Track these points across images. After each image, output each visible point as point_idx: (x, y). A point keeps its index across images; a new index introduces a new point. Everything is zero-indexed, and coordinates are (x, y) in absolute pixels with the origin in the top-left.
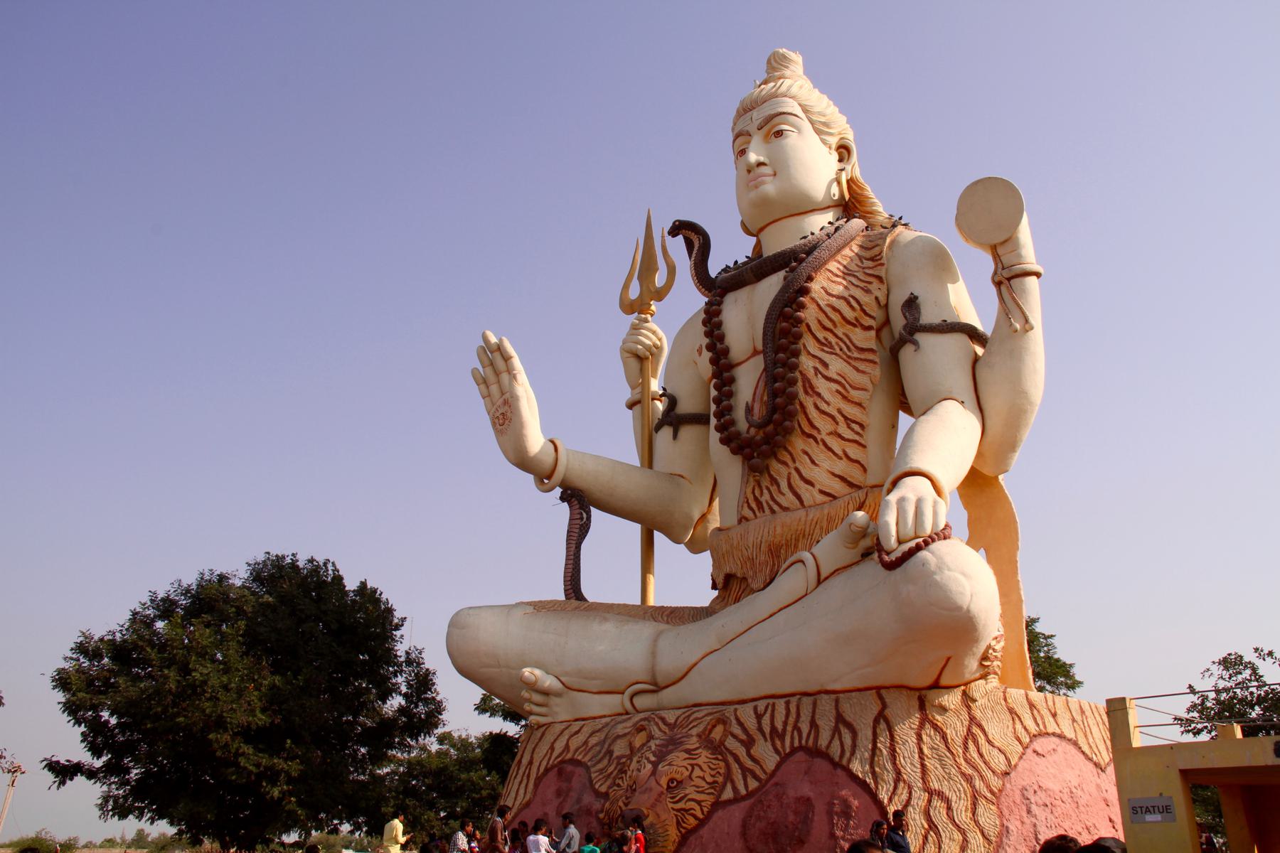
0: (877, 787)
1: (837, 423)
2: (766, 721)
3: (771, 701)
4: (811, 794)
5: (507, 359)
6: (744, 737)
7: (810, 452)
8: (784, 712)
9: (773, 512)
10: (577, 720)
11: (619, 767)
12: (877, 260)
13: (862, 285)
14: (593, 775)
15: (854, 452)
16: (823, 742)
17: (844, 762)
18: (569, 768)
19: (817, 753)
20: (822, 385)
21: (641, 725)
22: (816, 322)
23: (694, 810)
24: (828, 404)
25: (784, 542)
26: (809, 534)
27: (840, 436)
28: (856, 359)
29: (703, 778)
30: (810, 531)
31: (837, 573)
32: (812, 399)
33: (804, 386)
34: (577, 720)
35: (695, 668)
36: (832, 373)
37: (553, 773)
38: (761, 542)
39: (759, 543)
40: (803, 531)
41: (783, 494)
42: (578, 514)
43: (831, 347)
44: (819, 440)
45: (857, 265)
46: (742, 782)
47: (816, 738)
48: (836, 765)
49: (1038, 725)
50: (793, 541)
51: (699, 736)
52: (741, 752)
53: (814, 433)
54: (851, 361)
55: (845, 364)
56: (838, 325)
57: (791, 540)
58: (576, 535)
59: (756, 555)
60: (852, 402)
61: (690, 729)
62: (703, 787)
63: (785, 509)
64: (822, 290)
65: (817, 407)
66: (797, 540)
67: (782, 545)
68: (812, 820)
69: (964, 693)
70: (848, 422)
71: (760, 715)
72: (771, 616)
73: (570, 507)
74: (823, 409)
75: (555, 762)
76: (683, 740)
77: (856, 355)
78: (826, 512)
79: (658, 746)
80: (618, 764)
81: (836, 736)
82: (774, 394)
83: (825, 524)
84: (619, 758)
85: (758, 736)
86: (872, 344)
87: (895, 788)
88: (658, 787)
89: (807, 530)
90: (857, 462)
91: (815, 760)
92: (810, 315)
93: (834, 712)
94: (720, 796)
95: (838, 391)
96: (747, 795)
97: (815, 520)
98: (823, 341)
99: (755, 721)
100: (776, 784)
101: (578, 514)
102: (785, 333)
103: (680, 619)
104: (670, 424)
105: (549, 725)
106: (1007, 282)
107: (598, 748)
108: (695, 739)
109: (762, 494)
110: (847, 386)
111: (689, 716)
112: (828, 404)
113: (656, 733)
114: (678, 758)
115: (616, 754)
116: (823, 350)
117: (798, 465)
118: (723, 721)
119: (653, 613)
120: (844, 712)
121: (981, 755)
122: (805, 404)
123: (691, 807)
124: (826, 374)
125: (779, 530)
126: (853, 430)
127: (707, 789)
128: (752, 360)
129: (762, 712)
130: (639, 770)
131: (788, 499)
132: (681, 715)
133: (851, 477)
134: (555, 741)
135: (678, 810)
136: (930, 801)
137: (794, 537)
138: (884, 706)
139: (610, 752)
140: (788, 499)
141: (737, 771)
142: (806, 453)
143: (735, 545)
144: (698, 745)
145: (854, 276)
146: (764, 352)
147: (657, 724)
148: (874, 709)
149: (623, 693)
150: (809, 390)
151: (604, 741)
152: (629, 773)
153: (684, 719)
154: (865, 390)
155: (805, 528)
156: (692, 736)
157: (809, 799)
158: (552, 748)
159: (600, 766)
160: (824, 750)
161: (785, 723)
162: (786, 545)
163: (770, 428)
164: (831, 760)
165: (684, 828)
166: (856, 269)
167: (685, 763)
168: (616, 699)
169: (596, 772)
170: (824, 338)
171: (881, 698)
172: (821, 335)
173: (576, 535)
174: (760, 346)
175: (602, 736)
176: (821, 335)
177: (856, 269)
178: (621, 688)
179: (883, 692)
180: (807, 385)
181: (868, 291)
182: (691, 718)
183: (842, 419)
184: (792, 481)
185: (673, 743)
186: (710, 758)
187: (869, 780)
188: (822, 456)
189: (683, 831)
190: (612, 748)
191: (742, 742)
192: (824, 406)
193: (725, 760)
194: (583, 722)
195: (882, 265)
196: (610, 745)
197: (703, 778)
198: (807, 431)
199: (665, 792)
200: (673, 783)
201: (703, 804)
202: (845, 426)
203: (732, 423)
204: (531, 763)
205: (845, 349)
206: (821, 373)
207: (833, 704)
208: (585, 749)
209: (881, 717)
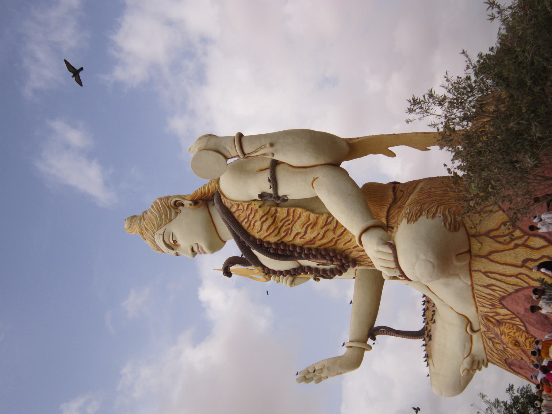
0: (521, 286)
1: (328, 230)
2: (487, 306)
6: (494, 314)
7: (345, 242)
13: (253, 213)
16: (498, 296)
19: (503, 298)
20: (310, 236)
22: (276, 237)
24: (319, 234)
28: (293, 217)
32: (317, 241)
33: (311, 244)
37: (512, 367)
43: (288, 229)
44: (338, 238)
45: (242, 212)
51: (494, 326)
53: (335, 240)
54: (295, 220)
55: (297, 223)
56: (276, 226)
64: (259, 234)
65: (321, 239)
69: (474, 236)
70: (327, 223)
72: (433, 293)
73: (378, 334)
74: (321, 237)
77: (291, 217)
86: (285, 210)
92: (273, 239)
93: (482, 287)
95: (312, 228)
98: (285, 233)
106: (246, 156)
108: (495, 328)
110: (308, 223)
112: (319, 234)
113: (492, 336)
115: (502, 349)
124: (303, 234)
136: (527, 267)
142: (345, 244)
145: (249, 215)
148: (481, 275)
149: (471, 336)
150: (312, 242)
154: (309, 216)
161: (487, 301)
169: (511, 357)
171: (476, 271)
180: (310, 243)
181: (257, 211)
182: (485, 325)
187: (517, 288)
188: (346, 237)
192: (320, 236)
193: (506, 323)
197: (515, 333)
198: (334, 244)
200: (517, 345)
205: (289, 222)
209: (485, 273)
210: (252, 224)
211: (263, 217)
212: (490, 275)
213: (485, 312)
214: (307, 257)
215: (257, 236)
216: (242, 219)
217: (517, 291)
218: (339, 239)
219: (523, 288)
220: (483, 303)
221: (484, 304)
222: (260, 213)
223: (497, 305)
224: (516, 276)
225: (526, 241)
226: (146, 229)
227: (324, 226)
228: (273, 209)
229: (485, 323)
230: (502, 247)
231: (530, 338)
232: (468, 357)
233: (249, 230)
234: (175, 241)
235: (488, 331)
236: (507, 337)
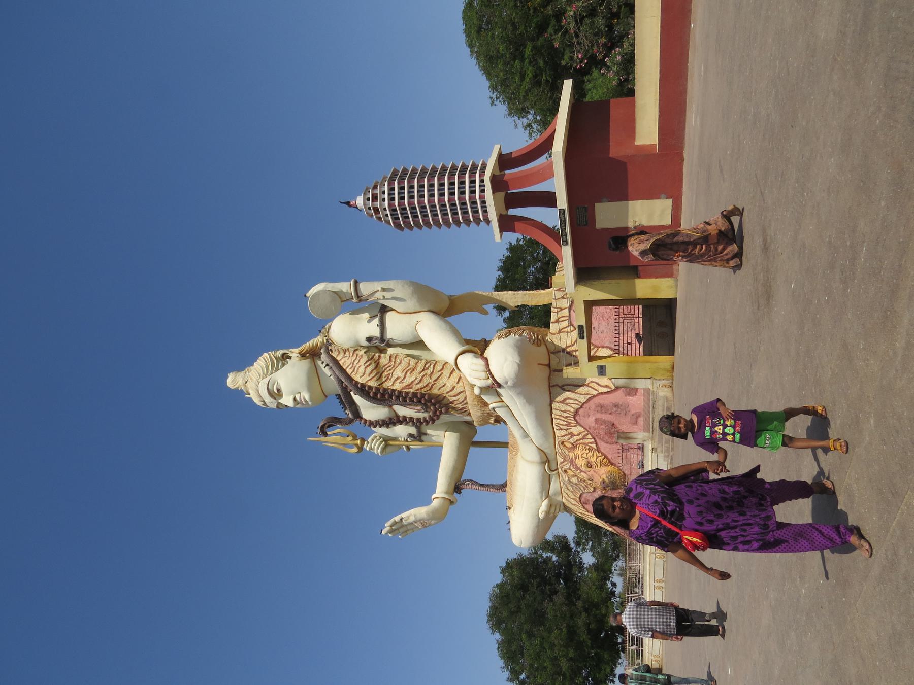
0: (591, 394)
1: (426, 374)
2: (563, 427)
4: (594, 418)
5: (395, 523)
6: (570, 436)
10: (562, 493)
15: (439, 367)
16: (572, 410)
18: (583, 500)
19: (576, 412)
20: (409, 380)
24: (416, 378)
29: (587, 454)
33: (409, 388)
36: (402, 376)
37: (586, 506)
43: (389, 374)
46: (589, 440)
47: (571, 412)
48: (582, 407)
51: (569, 452)
52: (576, 438)
53: (430, 385)
60: (416, 366)
65: (419, 383)
68: (605, 420)
69: (553, 353)
77: (393, 363)
80: (581, 481)
82: (411, 400)
85: (570, 431)
87: (592, 387)
92: (373, 384)
95: (411, 373)
96: (594, 439)
98: (386, 378)
102: (383, 395)
104: (420, 437)
108: (570, 454)
110: (408, 369)
112: (416, 378)
113: (567, 466)
115: (577, 482)
116: (391, 379)
117: (445, 392)
118: (563, 443)
122: (417, 388)
126: (428, 367)
135: (601, 465)
138: (557, 385)
139: (576, 484)
140: (462, 399)
142: (440, 389)
145: (354, 362)
147: (564, 465)
150: (410, 386)
157: (596, 419)
158: (575, 505)
159: (582, 488)
161: (564, 421)
164: (580, 408)
166: (350, 360)
167: (581, 460)
171: (554, 386)
172: (384, 379)
175: (569, 486)
176: (384, 379)
177: (349, 361)
179: (551, 385)
180: (407, 387)
181: (362, 356)
185: (572, 462)
187: (589, 396)
188: (441, 382)
189: (609, 464)
191: (571, 437)
192: (418, 381)
195: (348, 349)
197: (587, 454)
205: (390, 368)
212: (565, 387)
213: (562, 437)
214: (404, 404)
217: (588, 401)
218: (435, 384)
220: (561, 424)
221: (560, 426)
222: (365, 359)
223: (573, 423)
226: (251, 379)
228: (377, 355)
229: (561, 451)
231: (600, 456)
232: (546, 500)
233: (353, 376)
234: (279, 390)
235: (564, 462)
236: (581, 460)
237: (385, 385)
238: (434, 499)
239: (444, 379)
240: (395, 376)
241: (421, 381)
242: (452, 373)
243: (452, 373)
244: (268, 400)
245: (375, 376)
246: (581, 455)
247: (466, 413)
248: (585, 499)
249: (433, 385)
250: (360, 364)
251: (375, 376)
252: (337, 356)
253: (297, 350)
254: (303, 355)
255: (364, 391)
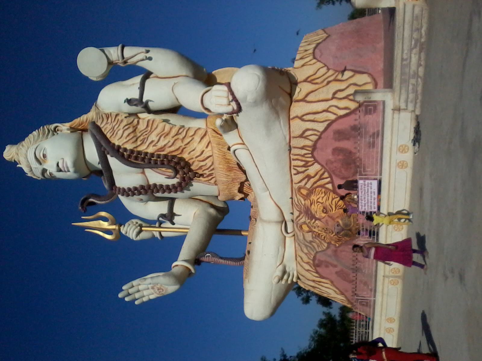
1: (178, 139)
3: (292, 167)
6: (306, 180)
8: (297, 161)
9: (213, 169)
11: (317, 238)
12: (108, 116)
14: (320, 250)
15: (191, 133)
16: (310, 143)
17: (319, 134)
18: (317, 262)
19: (314, 147)
20: (161, 144)
21: (300, 227)
22: (133, 144)
23: (336, 201)
25: (226, 165)
26: (224, 153)
27: (184, 138)
28: (151, 128)
30: (223, 153)
31: (240, 135)
32: (166, 148)
33: (161, 151)
34: (296, 259)
35: (276, 202)
36: (156, 139)
38: (226, 175)
39: (225, 176)
40: (223, 156)
41: (206, 164)
42: (207, 257)
43: (145, 139)
44: (184, 147)
48: (320, 138)
49: (310, 56)
50: (226, 160)
51: (305, 200)
52: (312, 180)
53: (181, 148)
54: (152, 131)
55: (153, 133)
57: (226, 161)
58: (216, 259)
59: (231, 177)
60: (170, 131)
61: (302, 204)
62: (326, 198)
63: (213, 164)
64: (119, 140)
66: (226, 159)
67: (228, 165)
70: (178, 133)
71: (297, 172)
72: (256, 166)
75: (314, 268)
76: (306, 207)
77: (149, 128)
78: (215, 145)
79: (308, 218)
80: (316, 238)
81: (307, 137)
82: (162, 163)
83: (220, 146)
84: (313, 238)
85: (306, 173)
88: (325, 218)
89: (222, 154)
90: (195, 132)
91: (317, 147)
92: (129, 146)
93: (298, 138)
94: (330, 190)
95: (164, 137)
97: (219, 150)
98: (141, 142)
99: (300, 174)
100: (326, 164)
101: (207, 257)
103: (256, 213)
105: (298, 272)
107: (309, 248)
108: (306, 202)
109: (205, 174)
110: (162, 133)
111: (297, 205)
112: (169, 142)
113: (303, 220)
114: (314, 208)
115: (311, 239)
117: (194, 157)
118: (300, 188)
119: (252, 225)
120: (298, 134)
121: (320, 77)
123: (334, 202)
125: (221, 166)
126: (182, 132)
127: (327, 195)
128: (147, 174)
129: (296, 171)
130: (318, 226)
131: (208, 162)
132: (296, 208)
133: (202, 134)
134: (304, 269)
135: (336, 208)
136: (336, 98)
137: (225, 160)
138: (297, 117)
139: (311, 242)
140: (208, 162)
141: (320, 182)
142: (190, 153)
143: (226, 187)
144: (309, 200)
146: (143, 168)
147: (299, 220)
149: (285, 237)
151: (306, 246)
152: (320, 232)
153: (298, 207)
154: (165, 126)
155: (221, 155)
156: (305, 203)
158: (308, 270)
159: (316, 246)
160: (313, 143)
161: (302, 161)
162: (228, 163)
163: (178, 167)
165: (343, 206)
167: (316, 205)
168: (288, 240)
169: (319, 249)
170: (140, 141)
171: (294, 118)
172: (139, 143)
173: (216, 259)
174: (140, 170)
175: (303, 246)
177: (111, 126)
178: (283, 237)
179: (291, 117)
181: (122, 121)
182: (297, 204)
183: (176, 136)
184: (201, 160)
186: (315, 195)
187: (326, 123)
190: (309, 241)
191: (308, 181)
192: (170, 144)
194: (297, 256)
196: (308, 242)
197: (323, 197)
199: (327, 214)
200: (324, 211)
201: (333, 197)
202: (180, 135)
203: (173, 185)
204: (314, 281)
206: (155, 144)
207: (295, 139)
208: (309, 254)
209: (301, 118)
210: (115, 133)
211: (126, 125)
212: (305, 117)
215: (117, 143)
216: (108, 131)
219: (333, 122)
224: (326, 111)
225: (337, 76)
227: (175, 135)
229: (298, 201)
230: (317, 86)
232: (281, 266)
234: (44, 156)
237: (140, 149)
238: (174, 267)
239: (194, 144)
240: (150, 140)
241: (173, 144)
242: (202, 138)
243: (202, 138)
244: (34, 164)
245: (131, 139)
246: (317, 200)
247: (212, 181)
248: (319, 260)
249: (185, 148)
250: (119, 128)
251: (131, 139)
252: (101, 124)
253: (68, 125)
254: (73, 130)
255: (118, 152)
